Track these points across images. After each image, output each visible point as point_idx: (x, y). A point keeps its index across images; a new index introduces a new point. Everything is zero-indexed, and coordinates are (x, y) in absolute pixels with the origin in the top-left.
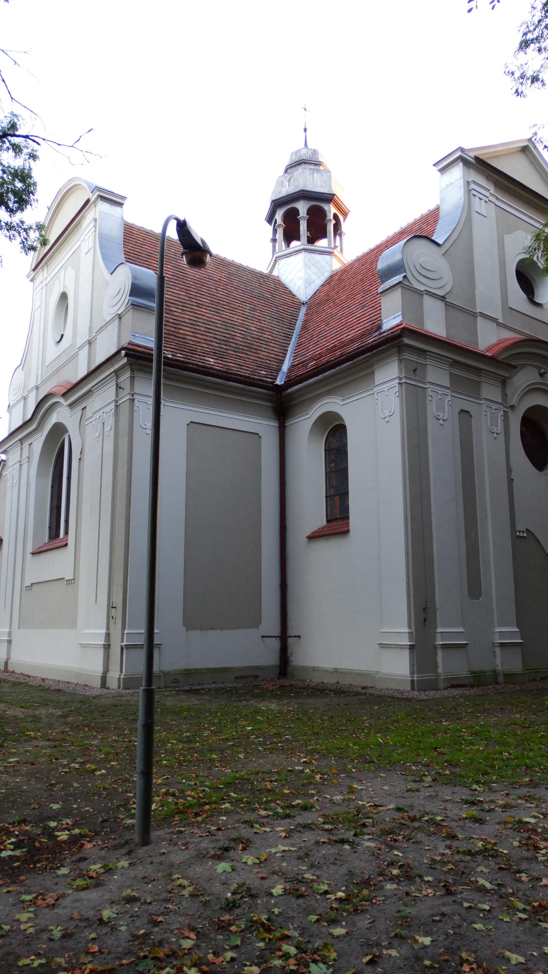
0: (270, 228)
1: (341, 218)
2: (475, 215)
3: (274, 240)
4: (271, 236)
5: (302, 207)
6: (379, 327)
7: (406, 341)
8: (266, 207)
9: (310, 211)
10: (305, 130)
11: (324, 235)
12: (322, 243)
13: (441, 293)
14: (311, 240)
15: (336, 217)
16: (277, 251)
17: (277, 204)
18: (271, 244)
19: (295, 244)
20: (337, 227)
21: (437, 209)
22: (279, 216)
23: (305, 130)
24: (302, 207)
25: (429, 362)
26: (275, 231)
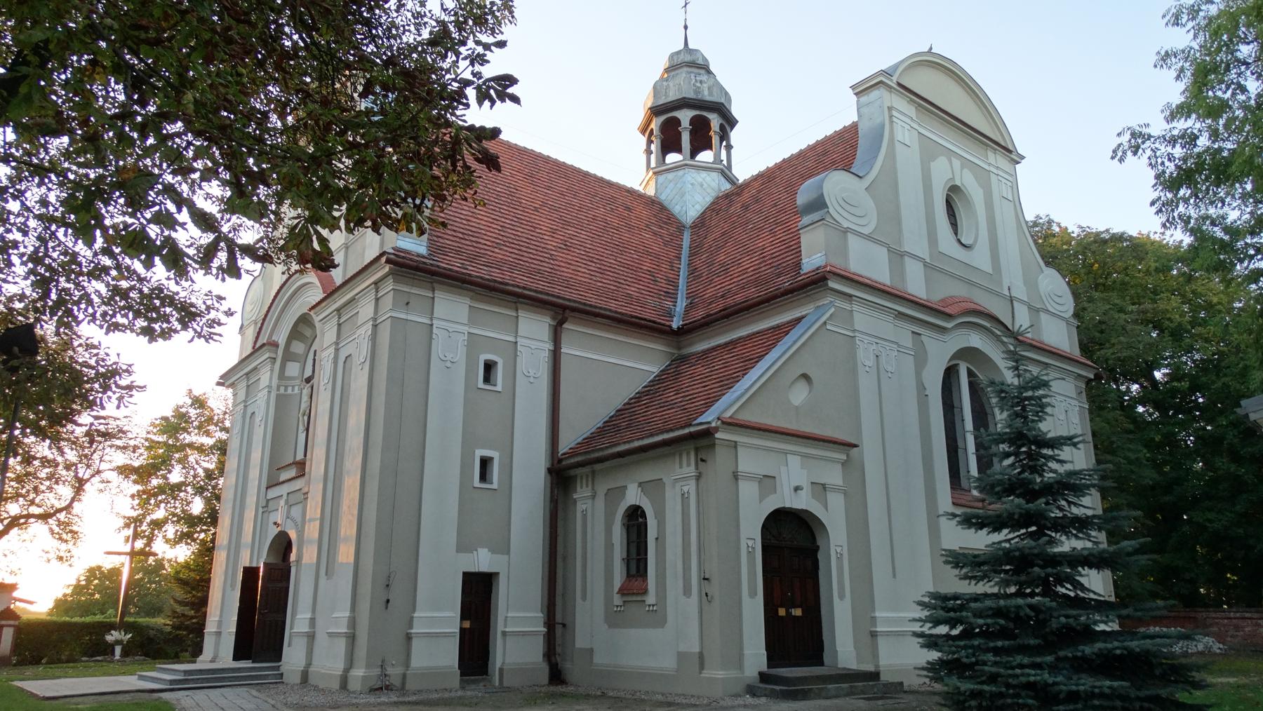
0: (643, 140)
1: (728, 129)
2: (898, 146)
3: (649, 152)
4: (645, 147)
5: (685, 116)
6: (798, 265)
7: (831, 284)
8: (640, 115)
9: (694, 121)
10: (686, 27)
11: (708, 146)
12: (706, 156)
13: (866, 231)
14: (693, 154)
15: (722, 127)
16: (653, 164)
17: (655, 111)
18: (644, 157)
19: (673, 158)
20: (724, 136)
21: (852, 130)
22: (655, 125)
23: (686, 27)
24: (685, 116)
25: (855, 308)
26: (650, 142)
